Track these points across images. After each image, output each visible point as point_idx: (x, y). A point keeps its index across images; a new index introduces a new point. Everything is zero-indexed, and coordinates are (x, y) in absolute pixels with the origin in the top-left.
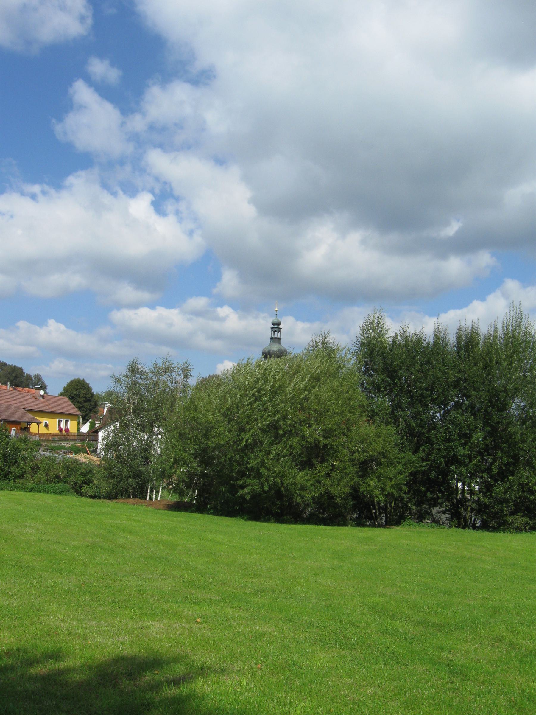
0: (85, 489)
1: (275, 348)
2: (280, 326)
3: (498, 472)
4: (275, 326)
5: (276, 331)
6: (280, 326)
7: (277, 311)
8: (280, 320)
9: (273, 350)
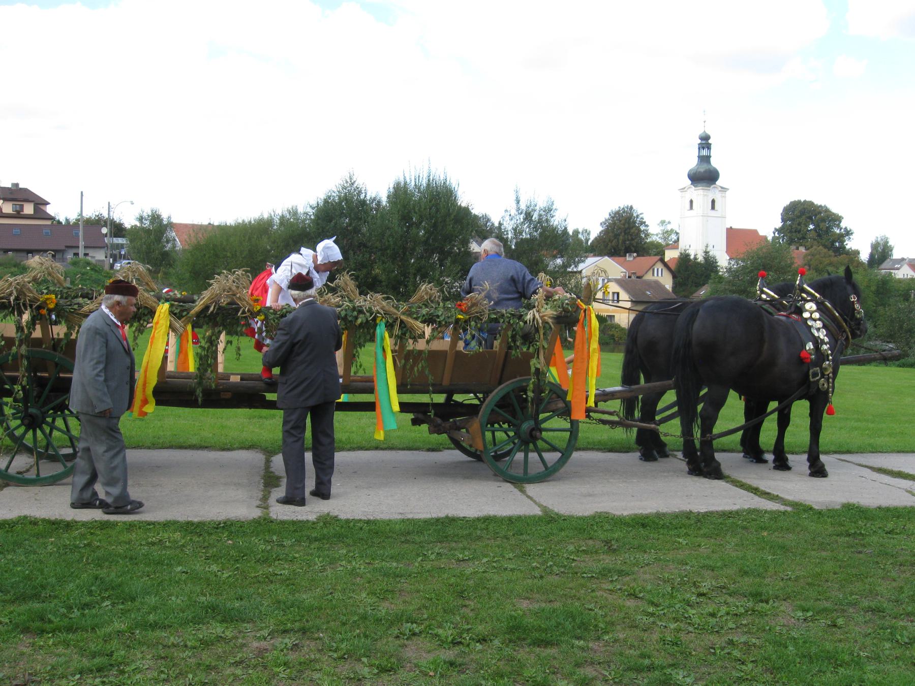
1: (702, 170)
2: (710, 141)
6: (710, 141)
8: (708, 132)
9: (700, 172)
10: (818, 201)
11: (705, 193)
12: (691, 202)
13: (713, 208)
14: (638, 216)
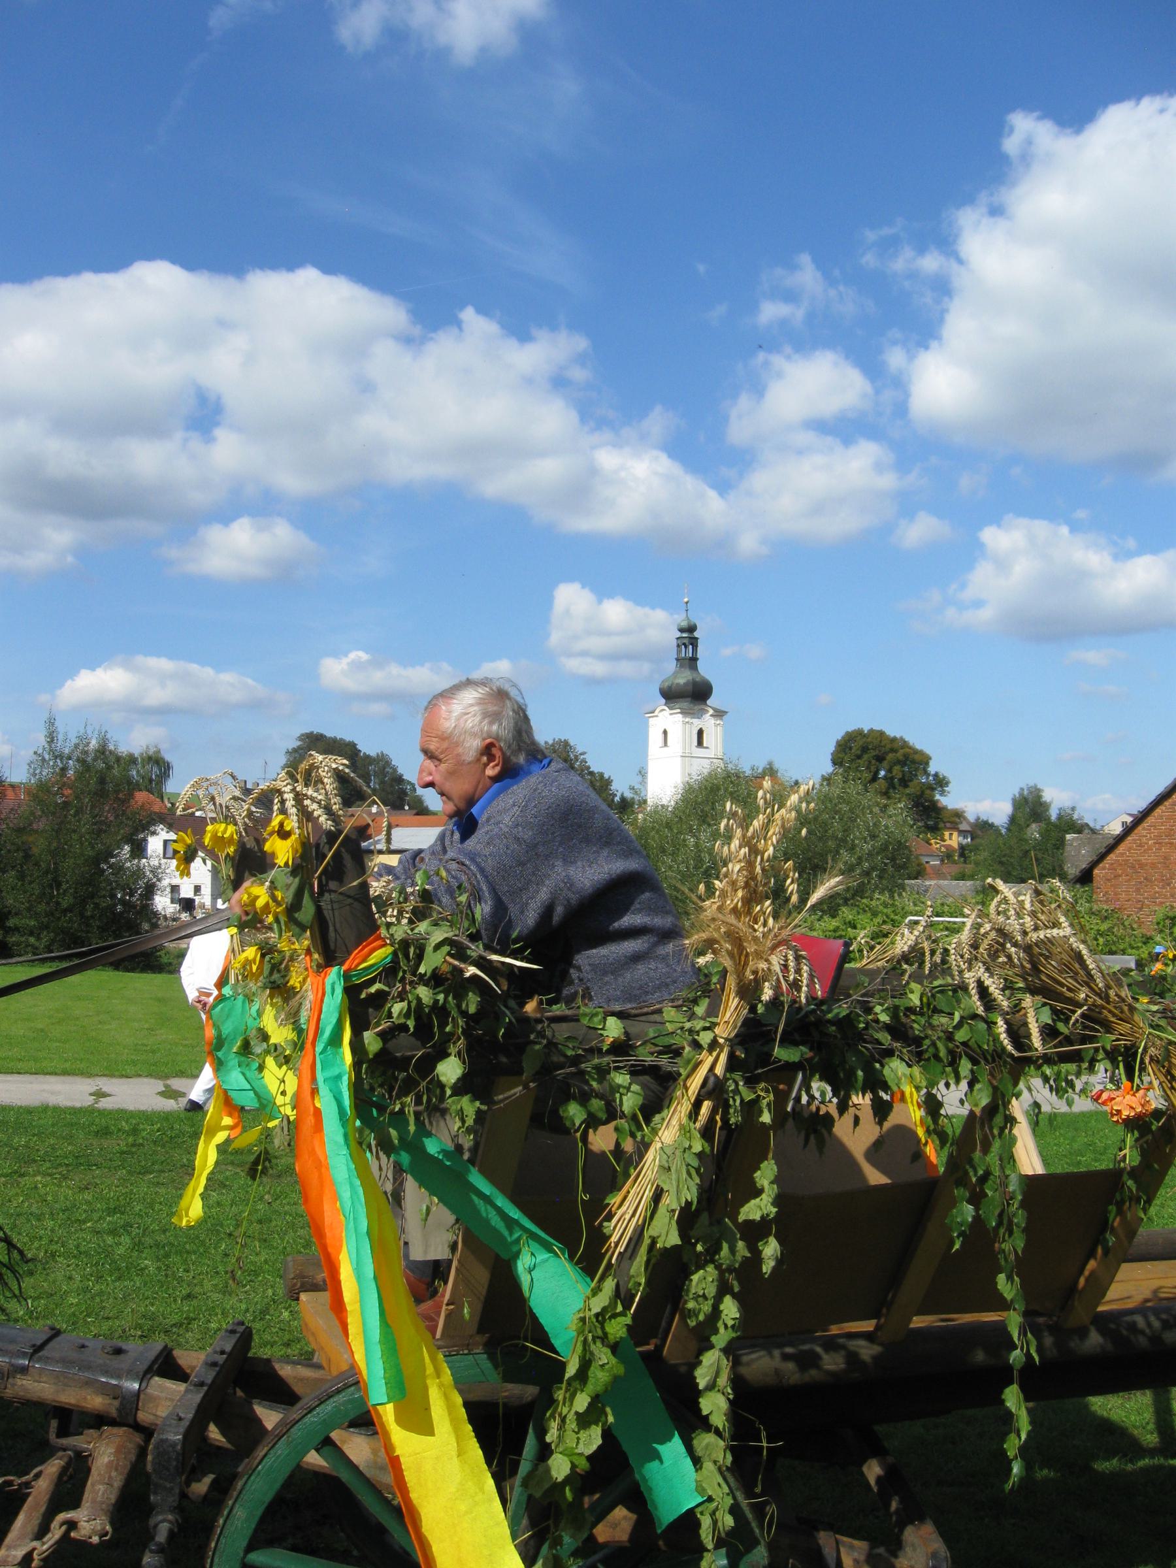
1: (681, 681)
2: (696, 634)
4: (685, 635)
6: (696, 634)
7: (687, 603)
8: (695, 620)
9: (678, 684)
10: (891, 732)
11: (687, 720)
12: (665, 732)
13: (700, 743)
14: (576, 757)
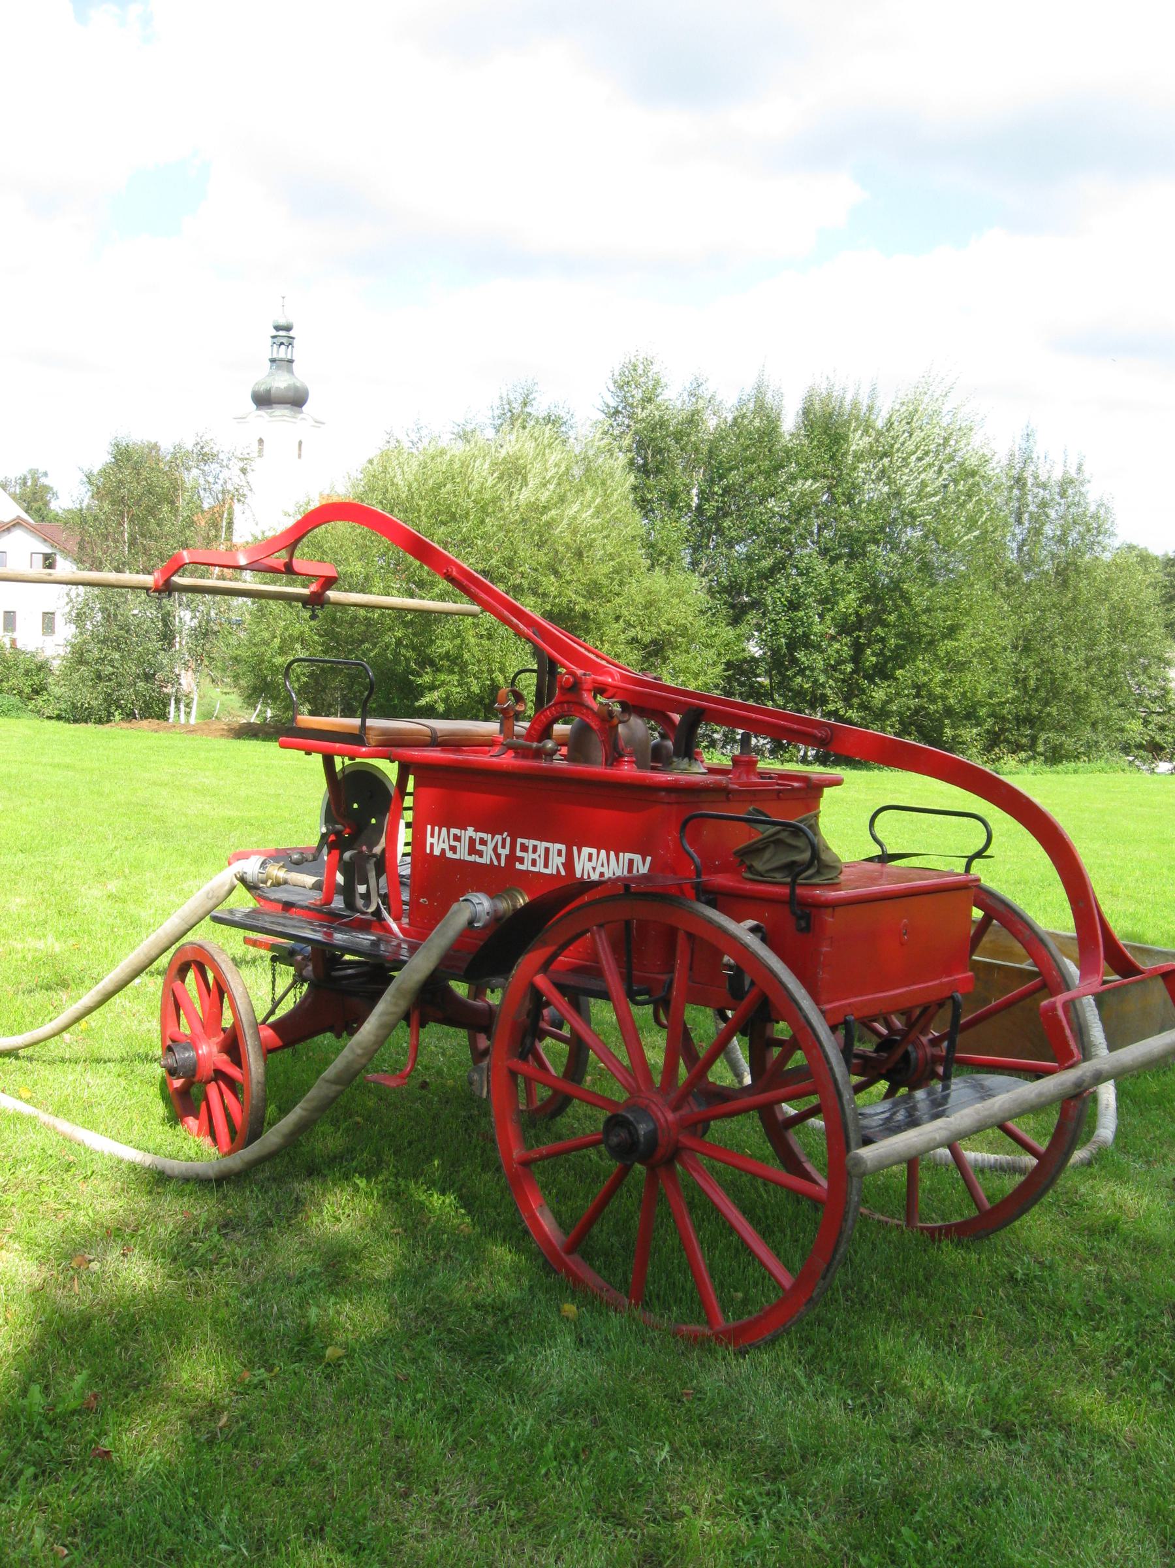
0: (39, 701)
1: (281, 382)
2: (292, 334)
3: (877, 663)
4: (282, 333)
5: (282, 344)
6: (292, 334)
